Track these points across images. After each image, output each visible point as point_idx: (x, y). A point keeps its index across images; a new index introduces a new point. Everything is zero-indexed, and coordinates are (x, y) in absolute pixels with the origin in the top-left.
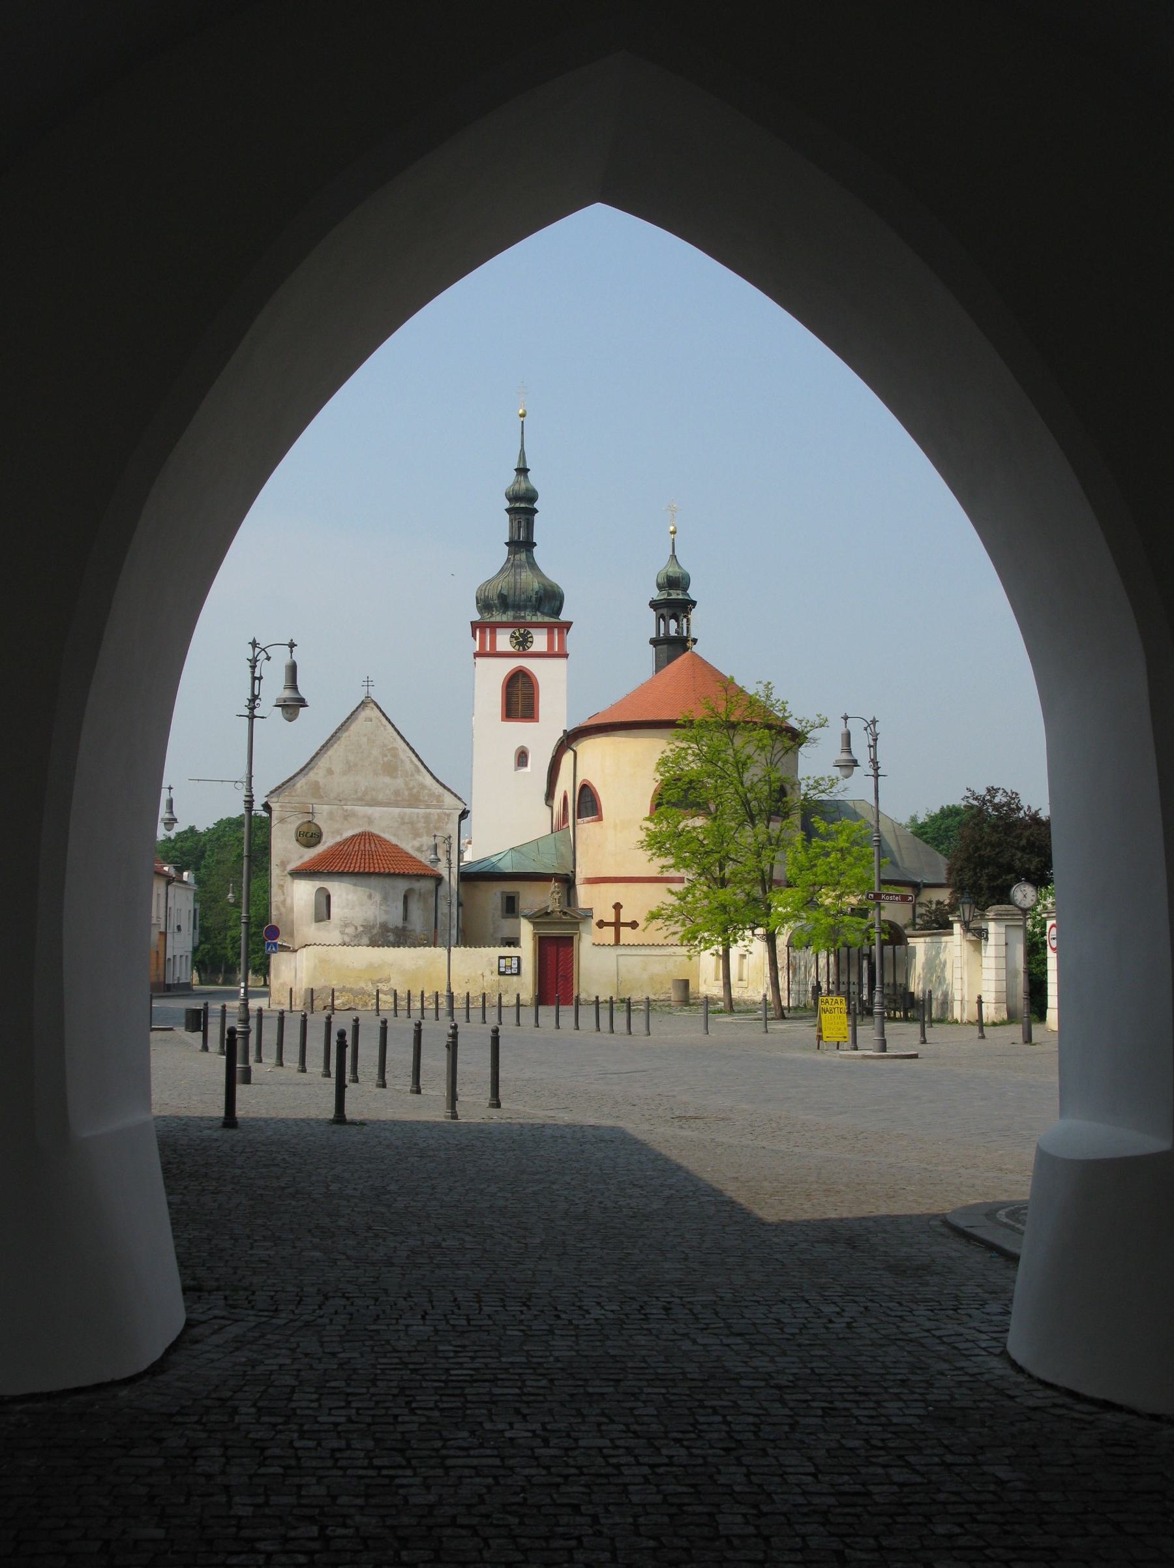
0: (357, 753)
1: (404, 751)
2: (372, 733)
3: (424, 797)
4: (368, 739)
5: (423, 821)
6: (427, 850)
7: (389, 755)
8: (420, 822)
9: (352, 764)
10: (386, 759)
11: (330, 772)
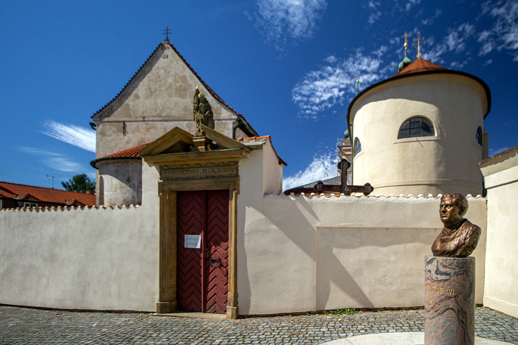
0: (157, 81)
1: (191, 78)
2: (168, 66)
4: (165, 71)
7: (180, 81)
9: (153, 90)
11: (137, 97)
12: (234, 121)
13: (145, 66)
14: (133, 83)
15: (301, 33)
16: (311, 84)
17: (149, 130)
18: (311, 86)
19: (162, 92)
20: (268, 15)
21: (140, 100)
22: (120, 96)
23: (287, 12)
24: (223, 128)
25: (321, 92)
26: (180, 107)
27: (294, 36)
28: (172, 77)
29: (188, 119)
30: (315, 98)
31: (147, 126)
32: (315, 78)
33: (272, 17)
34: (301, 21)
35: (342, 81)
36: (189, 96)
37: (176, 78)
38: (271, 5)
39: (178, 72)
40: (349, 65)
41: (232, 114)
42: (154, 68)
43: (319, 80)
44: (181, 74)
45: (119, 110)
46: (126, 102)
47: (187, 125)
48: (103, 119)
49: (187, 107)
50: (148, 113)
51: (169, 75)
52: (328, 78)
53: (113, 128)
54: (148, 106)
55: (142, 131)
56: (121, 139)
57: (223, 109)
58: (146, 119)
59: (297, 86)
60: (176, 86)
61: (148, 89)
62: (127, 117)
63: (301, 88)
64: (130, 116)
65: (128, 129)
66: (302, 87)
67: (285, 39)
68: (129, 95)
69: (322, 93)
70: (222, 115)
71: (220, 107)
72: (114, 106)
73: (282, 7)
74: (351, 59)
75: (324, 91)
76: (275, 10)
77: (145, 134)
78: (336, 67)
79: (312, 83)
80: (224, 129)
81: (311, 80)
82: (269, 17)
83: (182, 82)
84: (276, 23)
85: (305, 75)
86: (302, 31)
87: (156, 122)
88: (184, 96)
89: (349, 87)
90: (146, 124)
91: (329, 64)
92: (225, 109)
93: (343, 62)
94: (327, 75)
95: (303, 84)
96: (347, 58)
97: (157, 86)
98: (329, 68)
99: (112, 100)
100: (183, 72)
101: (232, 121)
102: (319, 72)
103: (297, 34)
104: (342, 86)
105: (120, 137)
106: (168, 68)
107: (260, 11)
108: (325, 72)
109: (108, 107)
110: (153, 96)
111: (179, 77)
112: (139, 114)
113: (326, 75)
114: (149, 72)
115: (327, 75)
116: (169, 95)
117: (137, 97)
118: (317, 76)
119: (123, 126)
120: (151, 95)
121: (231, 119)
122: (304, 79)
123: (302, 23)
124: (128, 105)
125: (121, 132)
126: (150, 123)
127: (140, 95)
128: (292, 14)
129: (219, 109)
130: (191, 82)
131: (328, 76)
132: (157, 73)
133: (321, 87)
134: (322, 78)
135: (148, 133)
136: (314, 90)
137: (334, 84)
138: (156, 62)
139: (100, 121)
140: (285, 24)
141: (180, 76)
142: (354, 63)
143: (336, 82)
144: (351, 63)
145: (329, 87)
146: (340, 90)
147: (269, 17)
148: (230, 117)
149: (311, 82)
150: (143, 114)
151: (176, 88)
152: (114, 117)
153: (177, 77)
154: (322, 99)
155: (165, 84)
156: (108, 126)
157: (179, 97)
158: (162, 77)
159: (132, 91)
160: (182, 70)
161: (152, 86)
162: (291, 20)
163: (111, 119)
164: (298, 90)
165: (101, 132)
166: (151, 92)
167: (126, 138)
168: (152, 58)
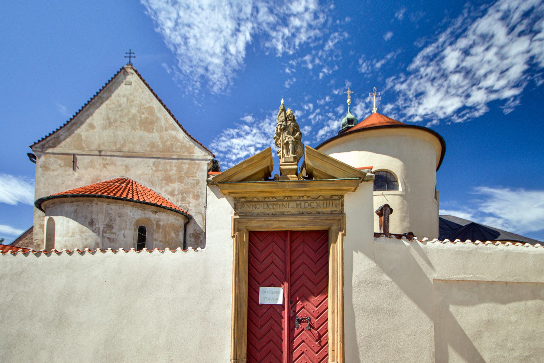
0: (117, 111)
2: (131, 94)
3: (176, 148)
4: (128, 99)
5: (175, 169)
6: (178, 194)
7: (145, 113)
8: (172, 170)
9: (112, 120)
10: (143, 116)
11: (92, 126)
12: (209, 162)
13: (102, 92)
14: (87, 110)
15: (219, 90)
16: (228, 141)
17: (107, 166)
18: (228, 143)
19: (123, 123)
20: (188, 69)
21: (95, 130)
22: (70, 124)
23: (206, 69)
24: (196, 169)
25: (237, 149)
26: (146, 143)
27: (213, 93)
28: (136, 107)
29: (155, 156)
30: (232, 155)
31: (104, 162)
32: (232, 136)
33: (192, 72)
34: (220, 79)
35: (258, 141)
36: (157, 131)
37: (141, 108)
38: (191, 61)
39: (144, 102)
40: (265, 126)
41: (206, 154)
42: (113, 95)
43: (235, 138)
44: (148, 105)
45: (68, 140)
46: (78, 131)
47: (154, 163)
48: (46, 150)
49: (154, 143)
50: (106, 146)
51: (132, 104)
52: (245, 136)
53: (60, 162)
54: (106, 138)
55: (97, 166)
56: (69, 175)
57: (196, 147)
58: (103, 153)
59: (214, 142)
60: (141, 117)
61: (105, 118)
62: (78, 149)
63: (218, 144)
64: (82, 148)
65: (79, 164)
66: (219, 143)
67: (203, 95)
68: (82, 123)
69: (239, 151)
70: (196, 155)
71: (194, 145)
72: (62, 135)
73: (202, 64)
74: (267, 120)
75: (241, 149)
76: (195, 66)
77: (101, 170)
78: (253, 127)
79: (229, 140)
80: (197, 170)
81: (228, 137)
82: (188, 71)
83: (149, 114)
84: (195, 79)
85: (223, 132)
86: (221, 89)
87: (115, 158)
88: (151, 131)
89: (265, 147)
90: (103, 159)
91: (246, 123)
92: (199, 147)
93: (260, 123)
94: (244, 133)
95: (220, 141)
96: (264, 119)
97: (118, 116)
98: (246, 128)
99: (59, 128)
100: (149, 103)
101: (207, 162)
102: (236, 130)
103: (216, 91)
104: (259, 146)
105: (68, 173)
106: (132, 97)
107: (179, 65)
108: (242, 130)
109: (53, 136)
110: (112, 127)
111: (144, 108)
112: (94, 147)
113: (244, 134)
114: (107, 98)
115: (244, 133)
116: (132, 127)
117: (92, 126)
118: (235, 134)
119: (73, 160)
120: (110, 126)
121: (206, 160)
122: (221, 136)
123: (221, 81)
124: (80, 136)
125: (70, 167)
126: (108, 158)
127: (95, 124)
128: (212, 72)
129: (192, 148)
130: (159, 115)
131: (245, 135)
132: (118, 101)
133: (238, 145)
134: (239, 136)
135: (105, 169)
136: (231, 147)
137: (251, 143)
138: (117, 88)
139: (42, 152)
140: (204, 80)
141: (146, 107)
142: (270, 124)
143: (253, 141)
144: (267, 124)
145: (246, 145)
146: (257, 149)
147: (188, 71)
148: (205, 157)
149: (228, 139)
150: (99, 147)
151: (141, 121)
152: (60, 148)
153: (142, 107)
154: (238, 156)
155: (127, 114)
156: (52, 159)
157: (144, 130)
158: (123, 106)
159: (86, 119)
160: (149, 100)
161: (110, 115)
162: (211, 77)
163: (57, 150)
164: (215, 146)
165: (42, 165)
166: (110, 123)
167: (76, 174)
168: (111, 83)
